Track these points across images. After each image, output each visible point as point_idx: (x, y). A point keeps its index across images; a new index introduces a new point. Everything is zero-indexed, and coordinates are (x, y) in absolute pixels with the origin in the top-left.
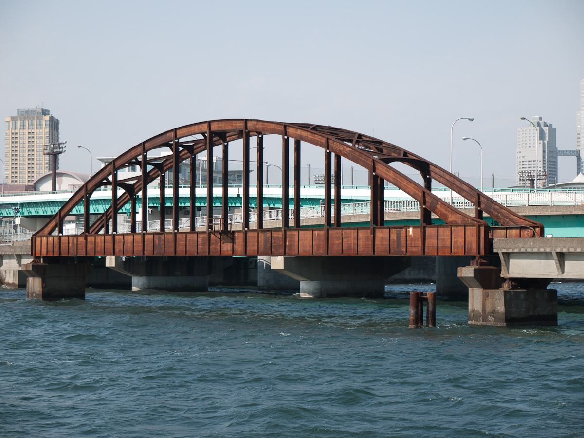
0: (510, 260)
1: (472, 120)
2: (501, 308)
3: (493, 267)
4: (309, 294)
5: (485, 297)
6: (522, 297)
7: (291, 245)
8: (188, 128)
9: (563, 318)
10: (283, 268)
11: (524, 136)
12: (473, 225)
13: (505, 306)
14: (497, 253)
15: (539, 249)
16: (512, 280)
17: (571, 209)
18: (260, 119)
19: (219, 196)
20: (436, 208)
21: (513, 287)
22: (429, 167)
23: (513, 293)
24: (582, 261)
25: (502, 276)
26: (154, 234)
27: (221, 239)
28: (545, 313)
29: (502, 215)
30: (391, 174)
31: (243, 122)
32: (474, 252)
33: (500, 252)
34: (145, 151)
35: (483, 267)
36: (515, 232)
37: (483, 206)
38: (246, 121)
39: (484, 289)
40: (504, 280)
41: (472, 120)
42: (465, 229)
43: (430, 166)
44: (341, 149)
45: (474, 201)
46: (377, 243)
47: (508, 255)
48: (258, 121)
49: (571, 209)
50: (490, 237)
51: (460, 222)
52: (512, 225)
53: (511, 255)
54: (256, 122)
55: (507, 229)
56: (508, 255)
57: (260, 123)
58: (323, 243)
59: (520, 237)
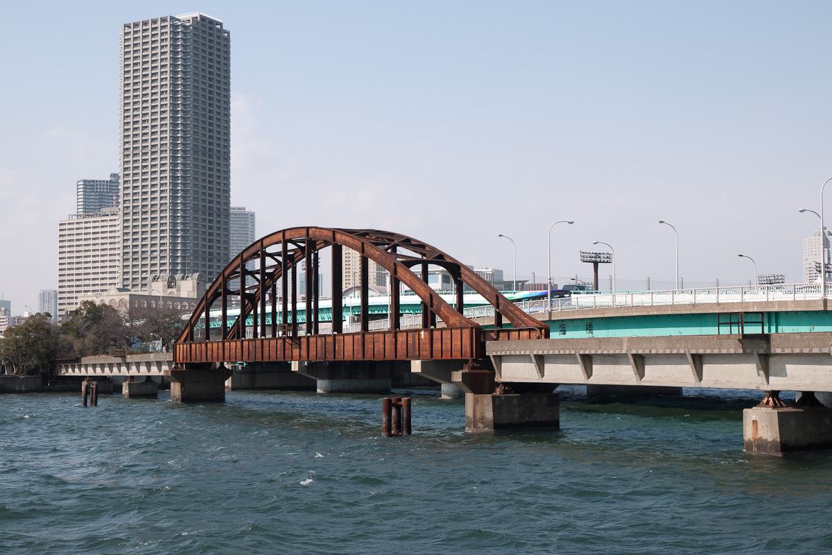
0: (503, 364)
1: (572, 223)
2: (489, 415)
3: (487, 371)
4: (449, 396)
5: (476, 402)
6: (515, 402)
7: (339, 350)
8: (270, 238)
9: (567, 421)
10: (420, 371)
11: (810, 247)
12: (468, 328)
13: (494, 411)
14: (489, 356)
15: (637, 351)
16: (505, 384)
17: (648, 310)
18: (319, 226)
19: (358, 305)
20: (441, 310)
21: (505, 392)
22: (460, 269)
23: (503, 398)
24: (828, 365)
25: (496, 380)
26: (249, 340)
27: (291, 345)
28: (545, 419)
29: (516, 316)
30: (408, 276)
31: (305, 229)
32: (468, 356)
33: (491, 355)
34: (244, 261)
35: (473, 371)
36: (526, 333)
37: (501, 308)
38: (308, 228)
39: (475, 393)
40: (498, 384)
41: (572, 223)
42: (461, 331)
43: (461, 268)
44: (373, 253)
45: (493, 302)
46: (398, 347)
47: (500, 358)
48: (316, 228)
49: (648, 310)
50: (482, 340)
51: (458, 325)
52: (523, 326)
53: (503, 358)
54: (314, 229)
55: (519, 330)
56: (500, 358)
57: (318, 230)
58: (358, 347)
59: (519, 339)
